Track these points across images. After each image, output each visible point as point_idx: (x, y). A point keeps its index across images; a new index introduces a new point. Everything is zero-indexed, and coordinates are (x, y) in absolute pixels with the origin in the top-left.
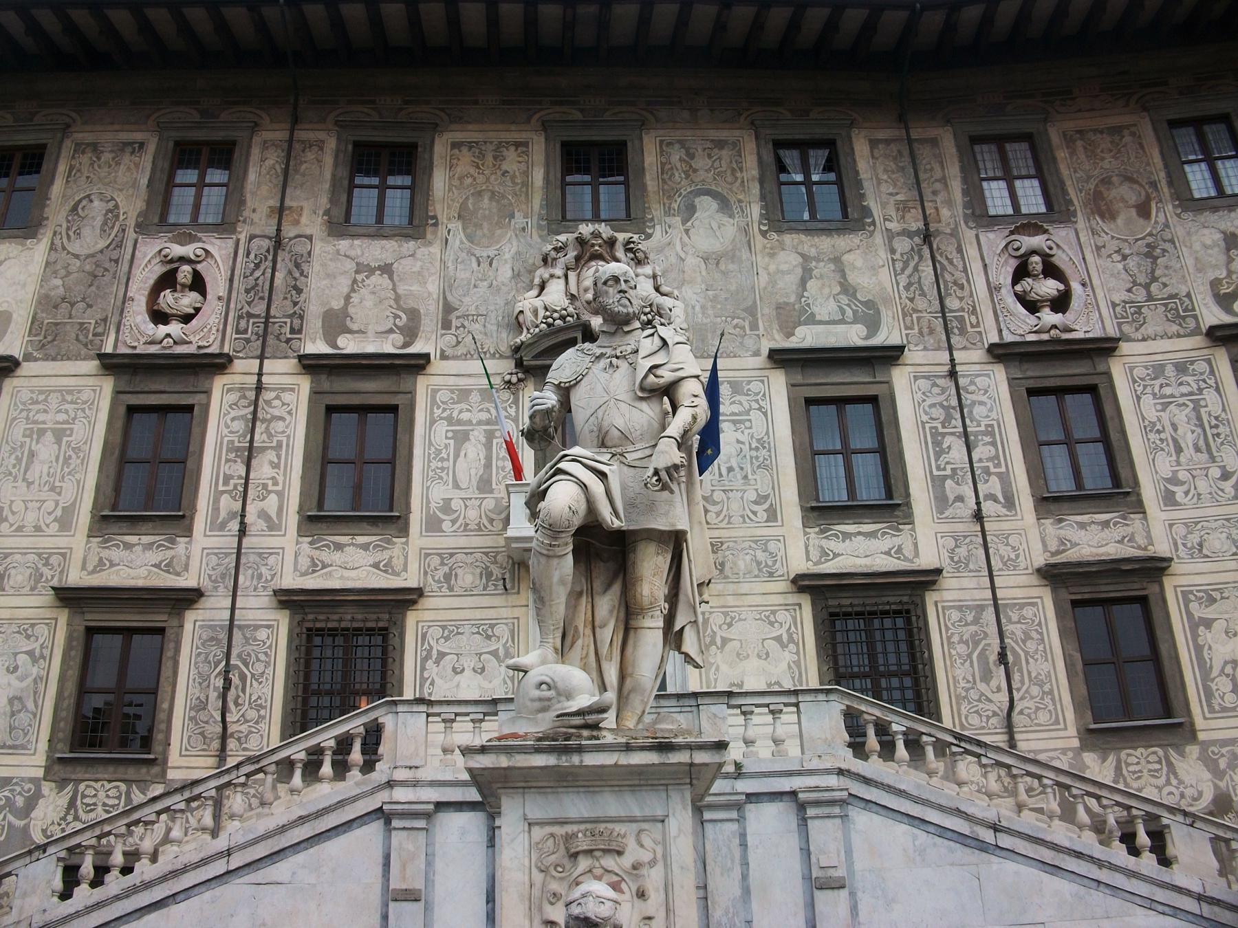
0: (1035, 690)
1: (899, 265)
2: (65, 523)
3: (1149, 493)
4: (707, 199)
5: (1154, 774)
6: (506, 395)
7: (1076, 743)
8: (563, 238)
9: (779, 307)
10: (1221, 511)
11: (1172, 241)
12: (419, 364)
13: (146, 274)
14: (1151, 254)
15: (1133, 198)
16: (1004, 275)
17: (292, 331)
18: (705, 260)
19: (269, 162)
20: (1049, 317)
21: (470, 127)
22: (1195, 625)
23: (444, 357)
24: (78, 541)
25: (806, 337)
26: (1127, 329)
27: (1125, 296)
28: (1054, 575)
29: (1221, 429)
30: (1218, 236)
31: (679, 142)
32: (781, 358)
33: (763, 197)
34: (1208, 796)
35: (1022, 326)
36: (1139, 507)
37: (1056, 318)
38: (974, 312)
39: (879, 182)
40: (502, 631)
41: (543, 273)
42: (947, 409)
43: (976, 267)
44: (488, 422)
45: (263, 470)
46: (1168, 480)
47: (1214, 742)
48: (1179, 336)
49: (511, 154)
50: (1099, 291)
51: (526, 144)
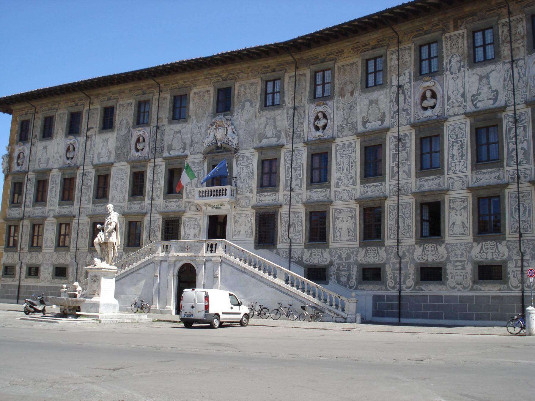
0: (298, 234)
1: (289, 118)
2: (124, 199)
3: (333, 182)
4: (248, 102)
5: (318, 255)
6: (202, 163)
7: (303, 247)
9: (259, 134)
10: (349, 188)
11: (356, 104)
12: (186, 156)
13: (134, 139)
14: (350, 109)
15: (350, 89)
16: (312, 120)
17: (162, 151)
18: (245, 121)
21: (198, 87)
23: (191, 154)
24: (126, 203)
25: (265, 142)
26: (339, 134)
27: (341, 123)
30: (368, 101)
31: (244, 85)
34: (328, 261)
36: (329, 187)
38: (303, 132)
39: (289, 91)
40: (198, 219)
41: (209, 131)
43: (307, 117)
44: (198, 171)
45: (156, 185)
46: (338, 179)
47: (333, 248)
48: (351, 135)
49: (206, 94)
50: (335, 123)
51: (208, 91)
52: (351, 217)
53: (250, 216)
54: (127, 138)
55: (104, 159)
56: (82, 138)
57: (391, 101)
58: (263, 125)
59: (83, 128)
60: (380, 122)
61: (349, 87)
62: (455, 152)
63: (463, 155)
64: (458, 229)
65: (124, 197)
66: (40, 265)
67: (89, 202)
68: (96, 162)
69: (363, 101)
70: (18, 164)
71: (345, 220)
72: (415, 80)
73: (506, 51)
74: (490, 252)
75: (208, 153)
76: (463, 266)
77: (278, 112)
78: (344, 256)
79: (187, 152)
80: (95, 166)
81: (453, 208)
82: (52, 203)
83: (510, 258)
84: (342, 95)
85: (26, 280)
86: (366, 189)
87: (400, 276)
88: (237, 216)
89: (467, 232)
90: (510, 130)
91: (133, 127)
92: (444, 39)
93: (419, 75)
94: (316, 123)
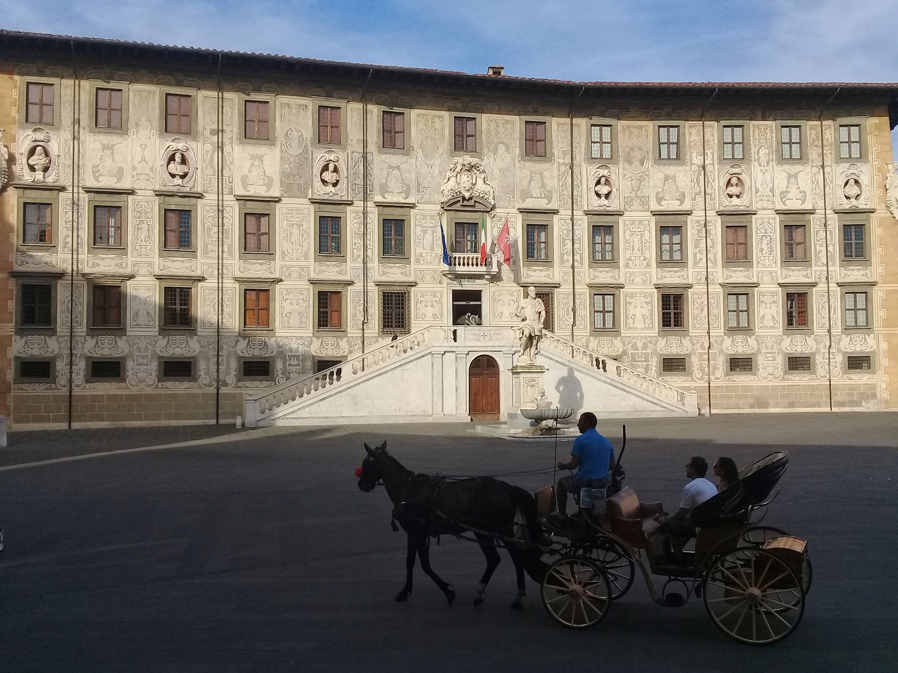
2: (306, 257)
3: (622, 263)
8: (456, 159)
9: (522, 191)
14: (640, 180)
19: (354, 119)
20: (603, 201)
22: (626, 303)
25: (530, 204)
28: (591, 286)
29: (648, 245)
32: (522, 211)
33: (520, 146)
34: (621, 350)
35: (597, 204)
37: (606, 202)
40: (438, 295)
42: (568, 231)
49: (437, 121)
52: (647, 303)
53: (515, 294)
54: (304, 160)
55: (261, 191)
56: (199, 144)
57: (692, 181)
58: (527, 180)
59: (200, 129)
60: (679, 202)
61: (638, 155)
62: (764, 247)
63: (771, 252)
64: (768, 322)
65: (307, 253)
66: (124, 359)
67: (231, 254)
68: (240, 191)
69: (657, 174)
70: (32, 168)
71: (639, 306)
72: (720, 163)
73: (814, 154)
74: (798, 344)
75: (449, 207)
76: (774, 357)
77: (545, 166)
78: (640, 345)
79: (411, 200)
80: (239, 199)
81: (763, 302)
82: (143, 251)
83: (818, 350)
84: (629, 161)
85: (88, 386)
86: (665, 274)
87: (709, 367)
88: (497, 294)
89: (777, 325)
90: (818, 232)
91: (313, 145)
92: (751, 126)
93: (722, 160)
94: (596, 189)
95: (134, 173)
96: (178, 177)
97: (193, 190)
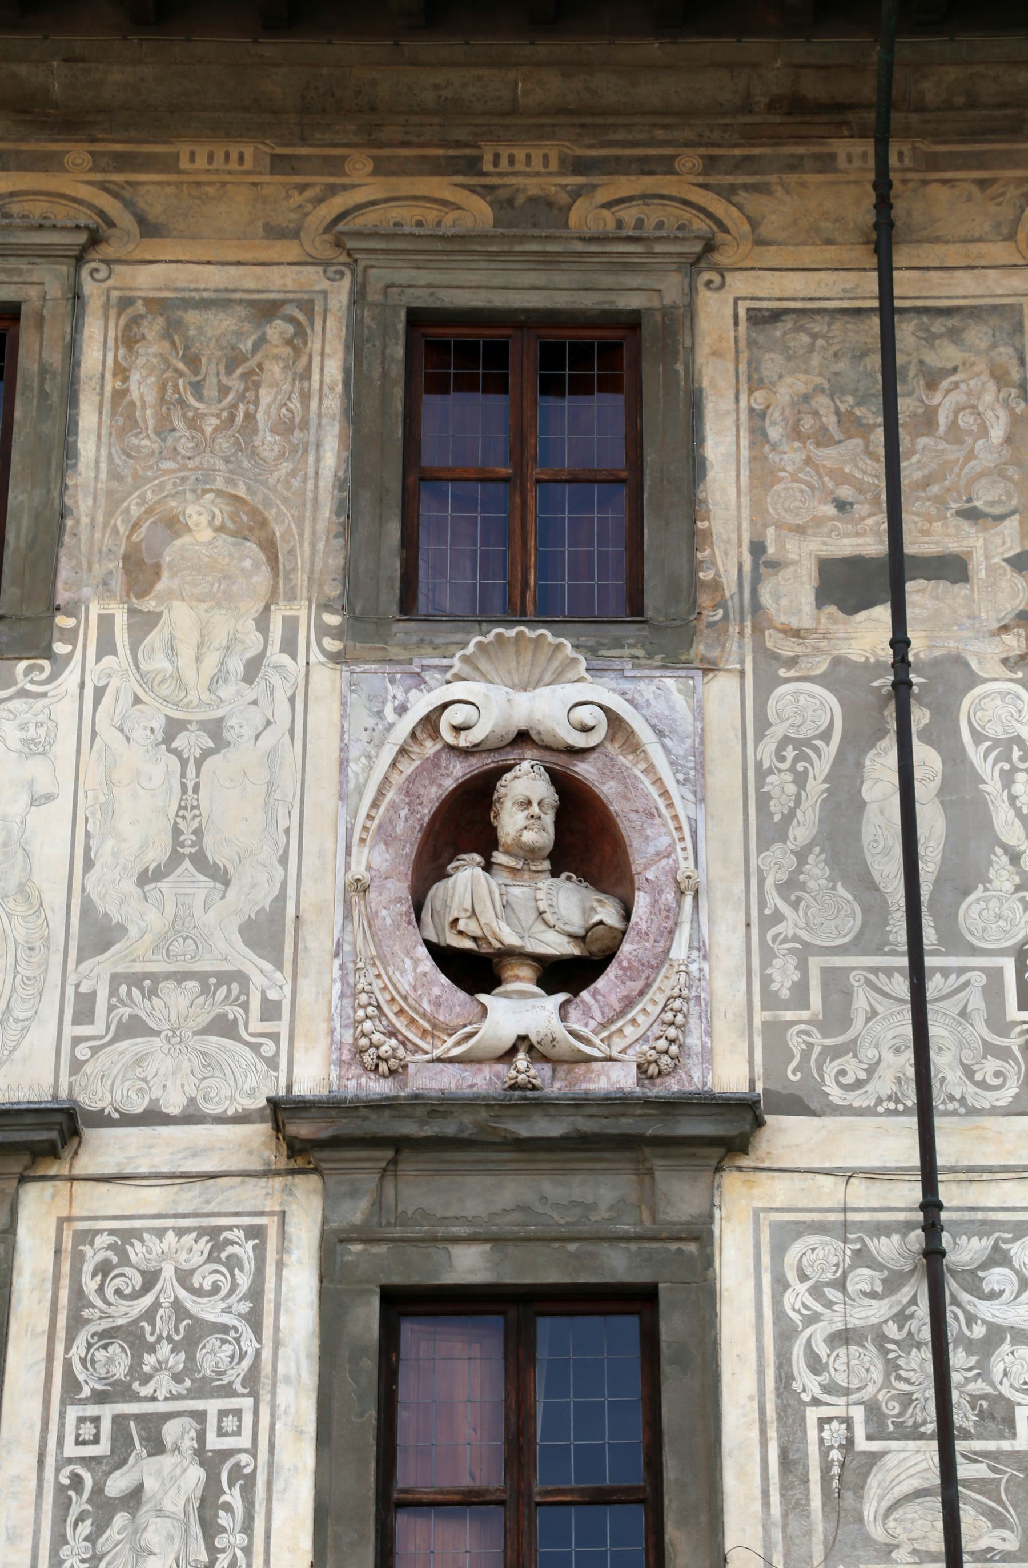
56: (724, 694)
59: (725, 560)
95: (97, 974)
96: (521, 980)
97: (673, 1086)
